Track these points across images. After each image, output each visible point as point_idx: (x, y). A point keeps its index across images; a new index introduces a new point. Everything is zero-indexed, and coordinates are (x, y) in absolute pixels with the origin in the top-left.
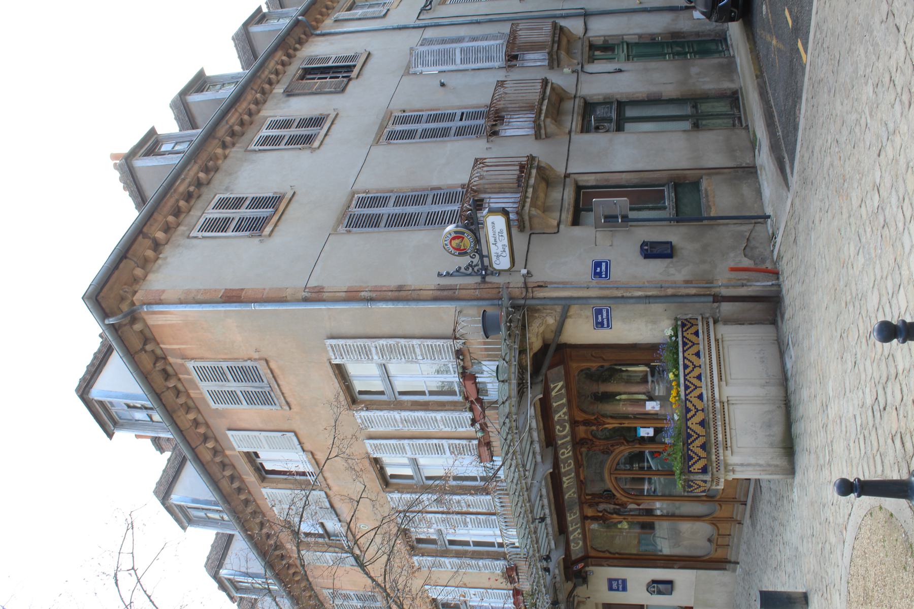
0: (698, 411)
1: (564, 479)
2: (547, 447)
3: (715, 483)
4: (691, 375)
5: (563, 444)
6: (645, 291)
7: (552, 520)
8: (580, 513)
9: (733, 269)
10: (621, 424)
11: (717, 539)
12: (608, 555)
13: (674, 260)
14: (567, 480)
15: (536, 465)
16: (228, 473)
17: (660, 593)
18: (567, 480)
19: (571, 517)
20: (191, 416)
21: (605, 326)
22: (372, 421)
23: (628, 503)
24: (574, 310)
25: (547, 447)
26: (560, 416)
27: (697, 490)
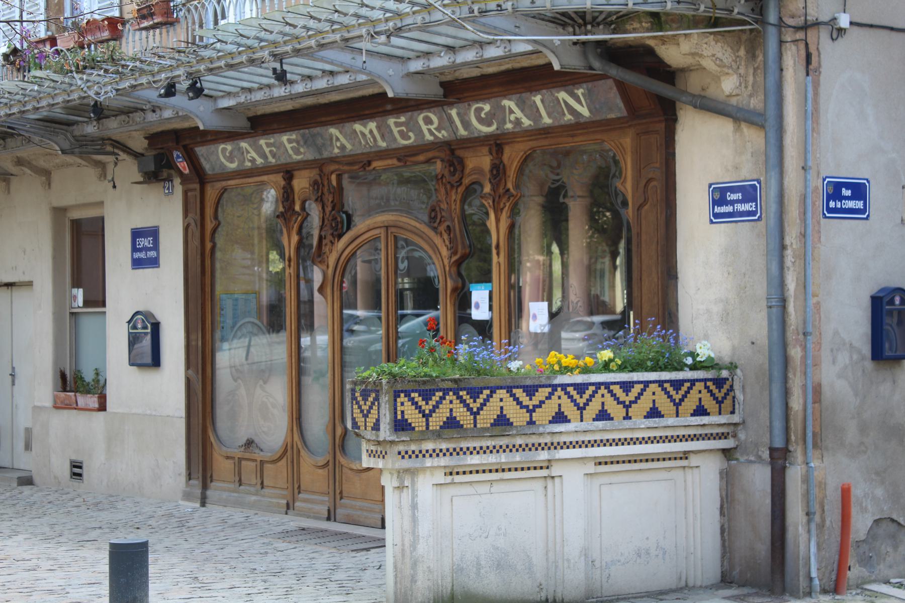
0: (531, 412)
1: (372, 125)
2: (443, 84)
3: (373, 448)
4: (608, 399)
5: (450, 118)
6: (796, 298)
7: (281, 99)
8: (299, 162)
9: (846, 493)
10: (498, 247)
11: (256, 460)
12: (209, 226)
13: (869, 364)
14: (371, 132)
15: (403, 59)
17: (133, 340)
18: (371, 132)
19: (290, 141)
21: (718, 210)
23: (325, 268)
24: (754, 137)
25: (443, 84)
26: (511, 112)
27: (356, 410)
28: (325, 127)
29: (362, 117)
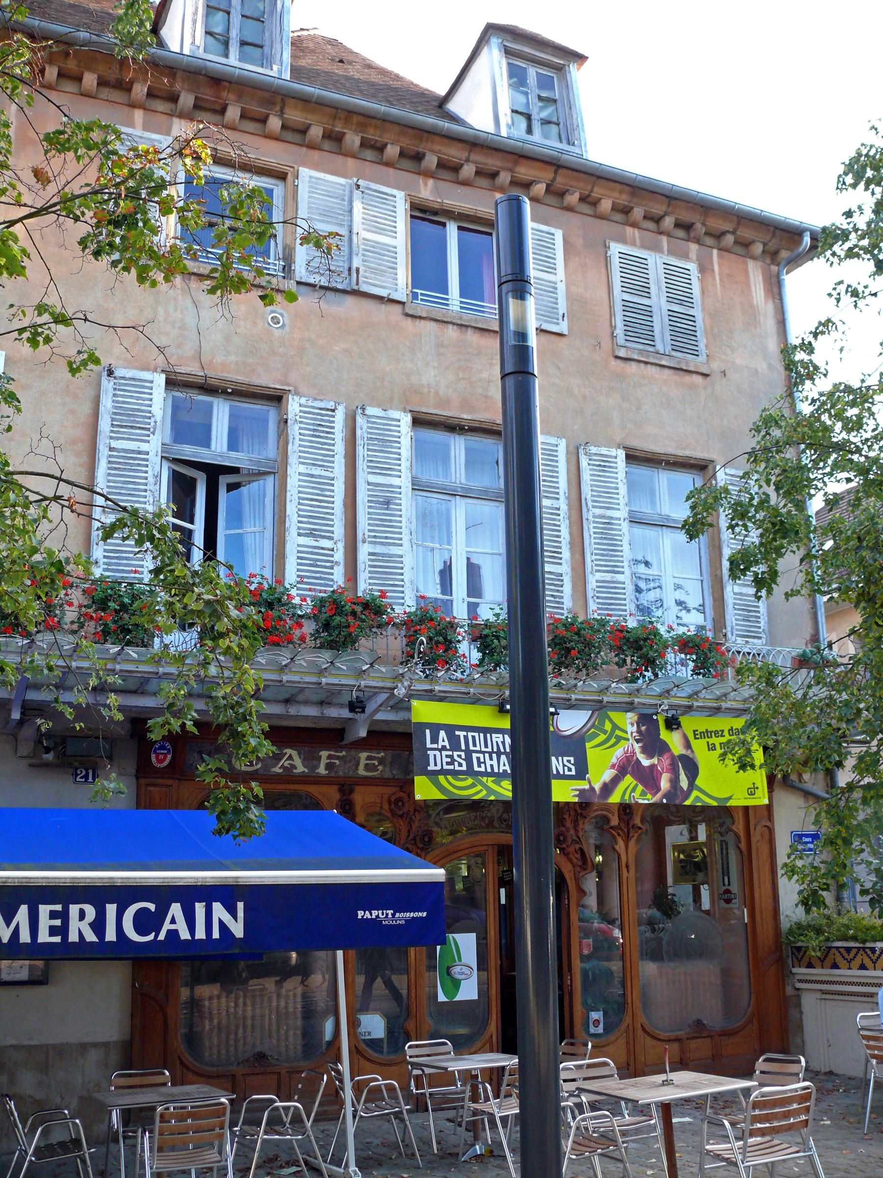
10: (627, 867)
16: (468, 170)
20: (606, 205)
22: (604, 471)
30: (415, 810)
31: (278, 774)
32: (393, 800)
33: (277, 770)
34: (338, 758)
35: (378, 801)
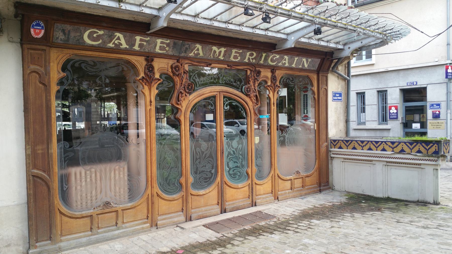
1: (223, 50)
14: (220, 52)
18: (220, 52)
21: (334, 98)
26: (285, 60)
27: (444, 149)
28: (196, 43)
29: (220, 45)
30: (184, 73)
31: (111, 48)
32: (174, 66)
33: (111, 45)
34: (145, 41)
35: (166, 67)
